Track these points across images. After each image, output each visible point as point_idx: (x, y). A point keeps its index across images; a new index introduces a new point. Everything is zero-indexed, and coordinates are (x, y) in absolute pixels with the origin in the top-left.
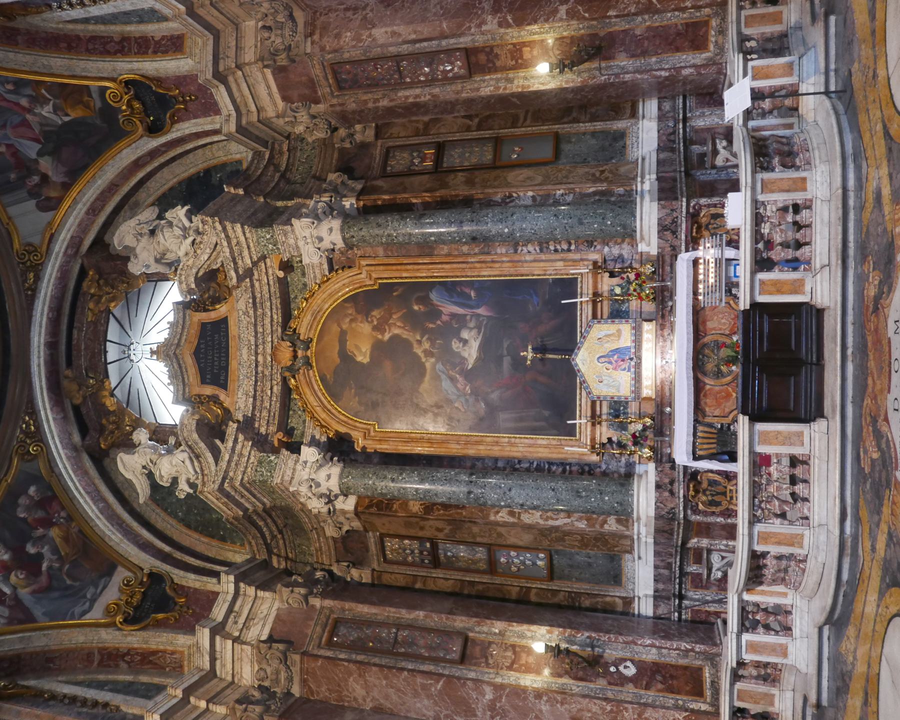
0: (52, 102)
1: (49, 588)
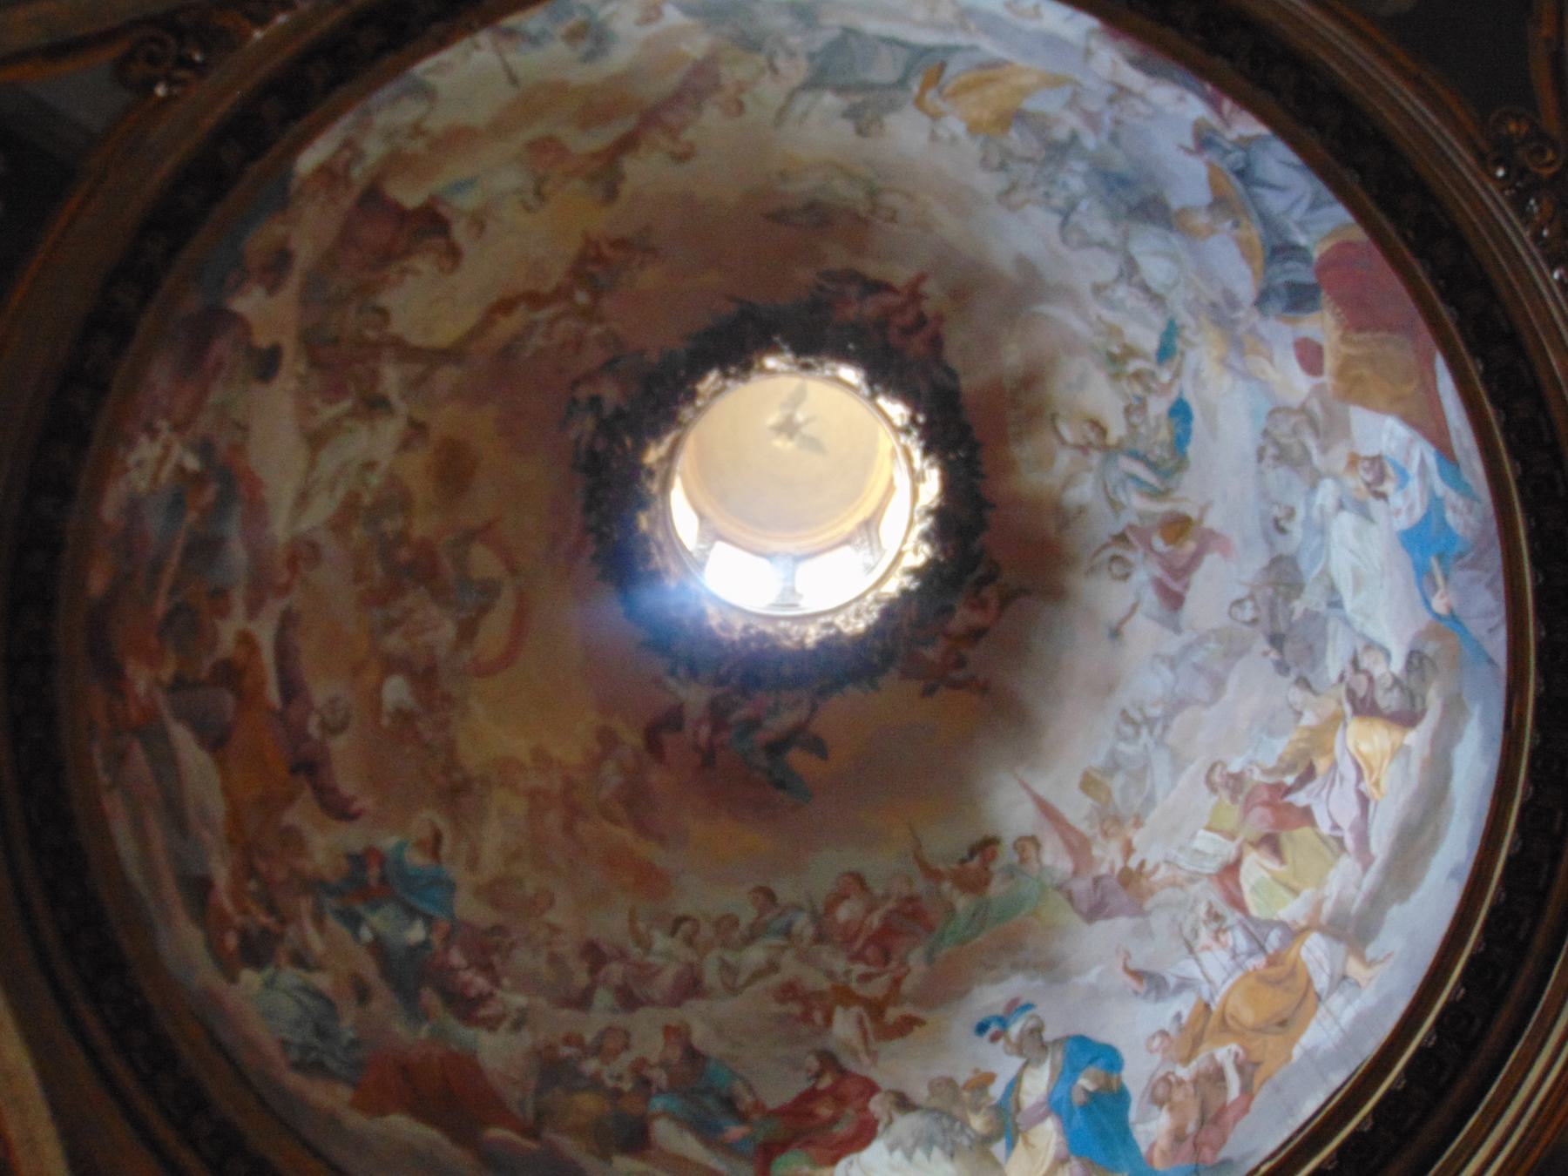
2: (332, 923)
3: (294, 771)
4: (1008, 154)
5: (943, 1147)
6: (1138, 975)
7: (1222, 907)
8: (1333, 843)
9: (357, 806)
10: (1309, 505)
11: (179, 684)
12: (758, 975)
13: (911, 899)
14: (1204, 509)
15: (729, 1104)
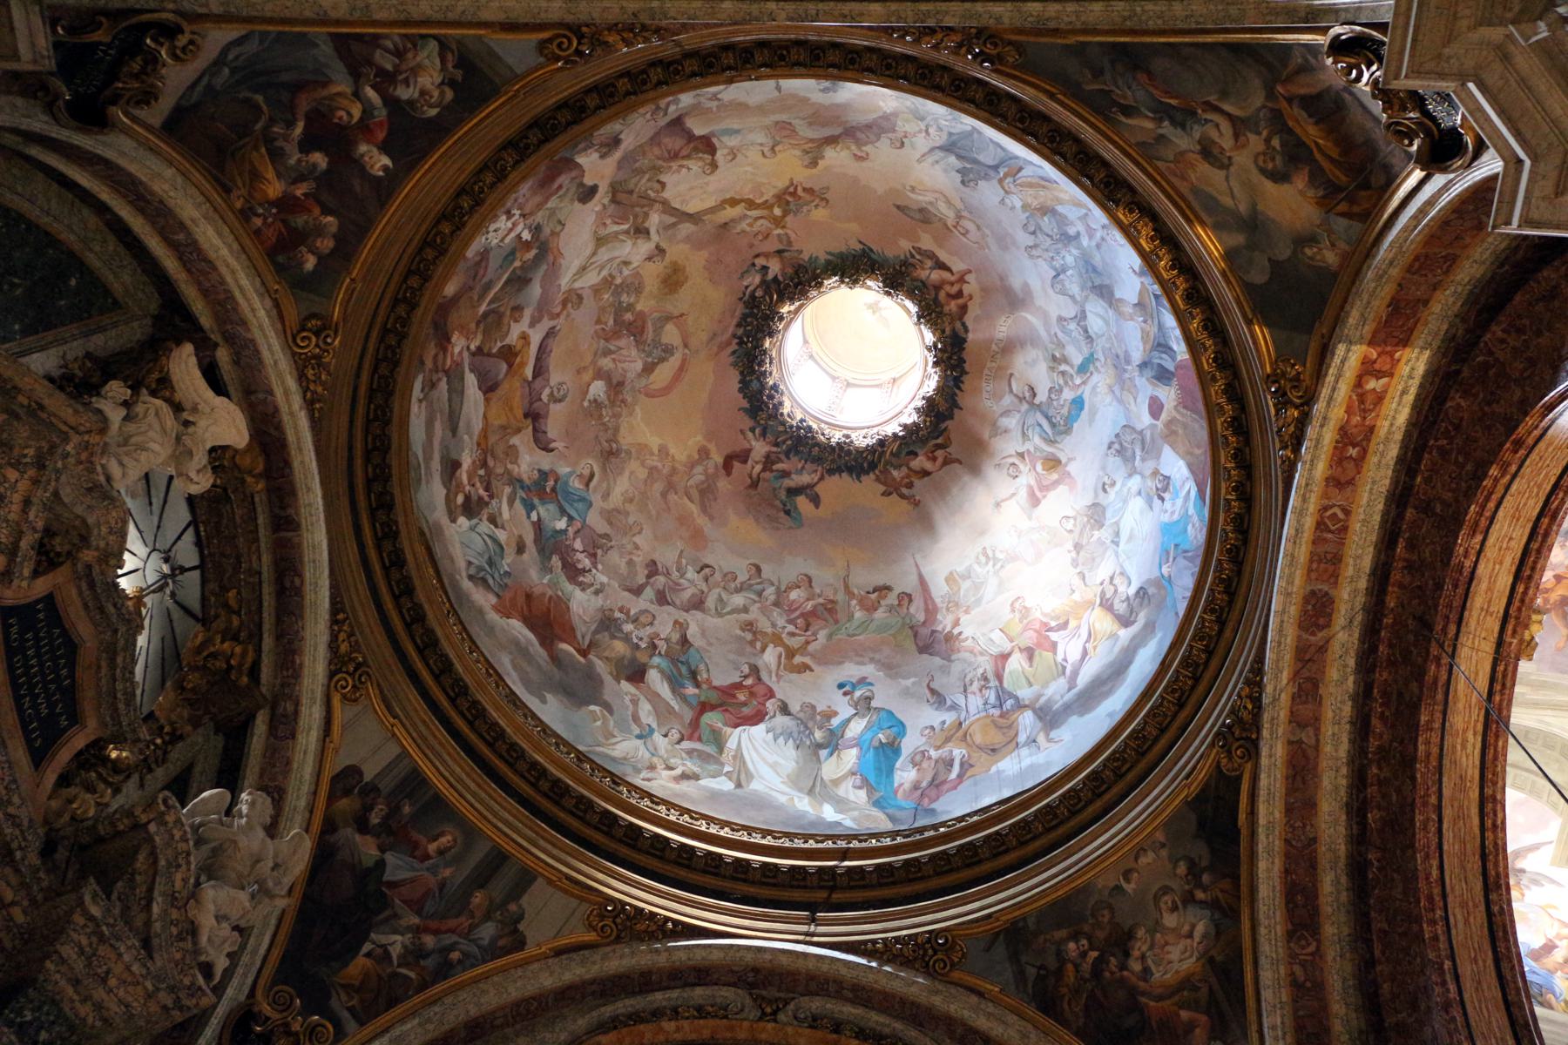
0: (395, 963)
1: (298, 87)
2: (518, 504)
3: (526, 416)
5: (795, 741)
6: (933, 691)
7: (990, 675)
9: (553, 445)
10: (1123, 485)
12: (735, 611)
13: (832, 602)
14: (1070, 460)
15: (694, 675)
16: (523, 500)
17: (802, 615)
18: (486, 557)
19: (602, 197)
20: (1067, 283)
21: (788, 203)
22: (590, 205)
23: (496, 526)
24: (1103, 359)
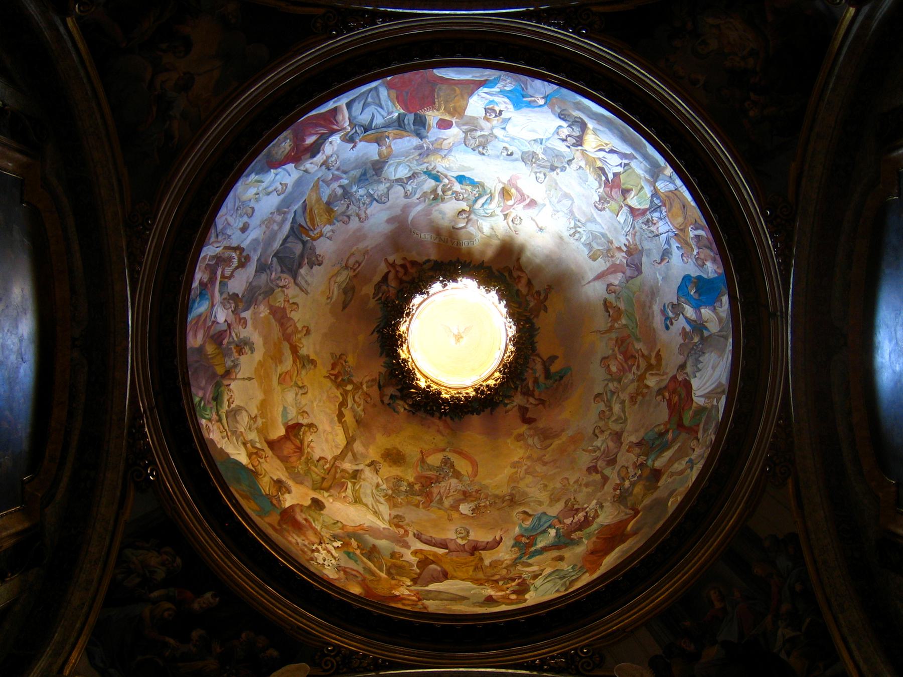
4: (343, 213)
6: (662, 260)
7: (645, 219)
8: (626, 168)
9: (498, 538)
10: (503, 141)
11: (415, 581)
12: (624, 411)
13: (616, 341)
14: (500, 182)
15: (662, 435)
16: (529, 558)
17: (626, 361)
18: (558, 581)
19: (323, 496)
20: (380, 193)
21: (343, 380)
22: (326, 504)
23: (541, 574)
24: (426, 165)
